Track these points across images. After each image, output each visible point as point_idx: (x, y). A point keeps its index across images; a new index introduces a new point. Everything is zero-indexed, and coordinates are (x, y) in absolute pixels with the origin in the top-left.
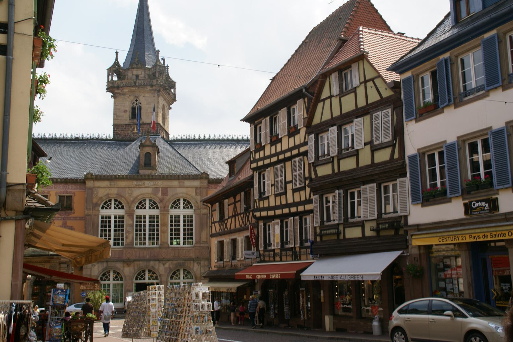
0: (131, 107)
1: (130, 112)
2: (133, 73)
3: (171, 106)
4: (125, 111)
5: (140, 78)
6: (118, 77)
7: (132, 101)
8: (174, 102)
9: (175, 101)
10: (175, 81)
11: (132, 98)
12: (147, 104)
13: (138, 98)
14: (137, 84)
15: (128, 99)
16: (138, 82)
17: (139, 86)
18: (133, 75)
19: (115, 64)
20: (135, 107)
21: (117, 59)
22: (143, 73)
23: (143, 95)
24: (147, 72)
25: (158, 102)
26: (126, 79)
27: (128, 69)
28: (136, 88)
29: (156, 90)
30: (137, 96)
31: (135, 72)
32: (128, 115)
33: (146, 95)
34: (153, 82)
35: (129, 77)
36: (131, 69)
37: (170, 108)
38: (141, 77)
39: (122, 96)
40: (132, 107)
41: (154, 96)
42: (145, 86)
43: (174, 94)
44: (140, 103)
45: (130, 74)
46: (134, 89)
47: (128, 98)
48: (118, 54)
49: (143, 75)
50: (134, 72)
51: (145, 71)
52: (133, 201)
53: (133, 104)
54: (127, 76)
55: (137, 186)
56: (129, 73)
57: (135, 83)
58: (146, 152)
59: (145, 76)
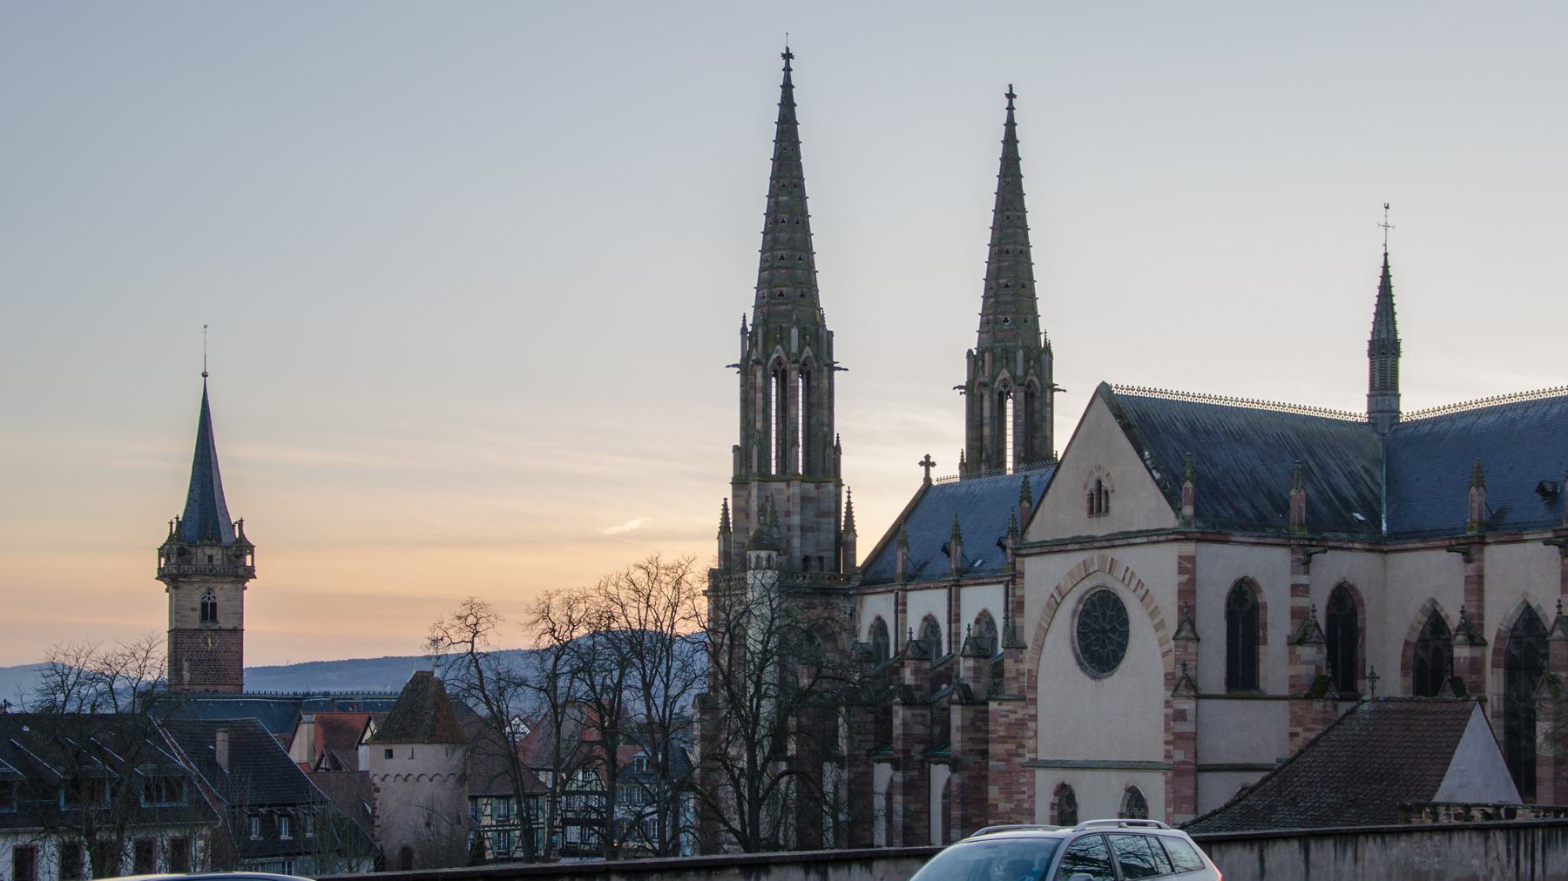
4: (194, 610)
5: (215, 562)
12: (227, 601)
18: (204, 555)
22: (220, 553)
31: (208, 551)
33: (226, 586)
39: (188, 587)
41: (237, 590)
44: (214, 597)
45: (200, 554)
49: (219, 557)
50: (206, 550)
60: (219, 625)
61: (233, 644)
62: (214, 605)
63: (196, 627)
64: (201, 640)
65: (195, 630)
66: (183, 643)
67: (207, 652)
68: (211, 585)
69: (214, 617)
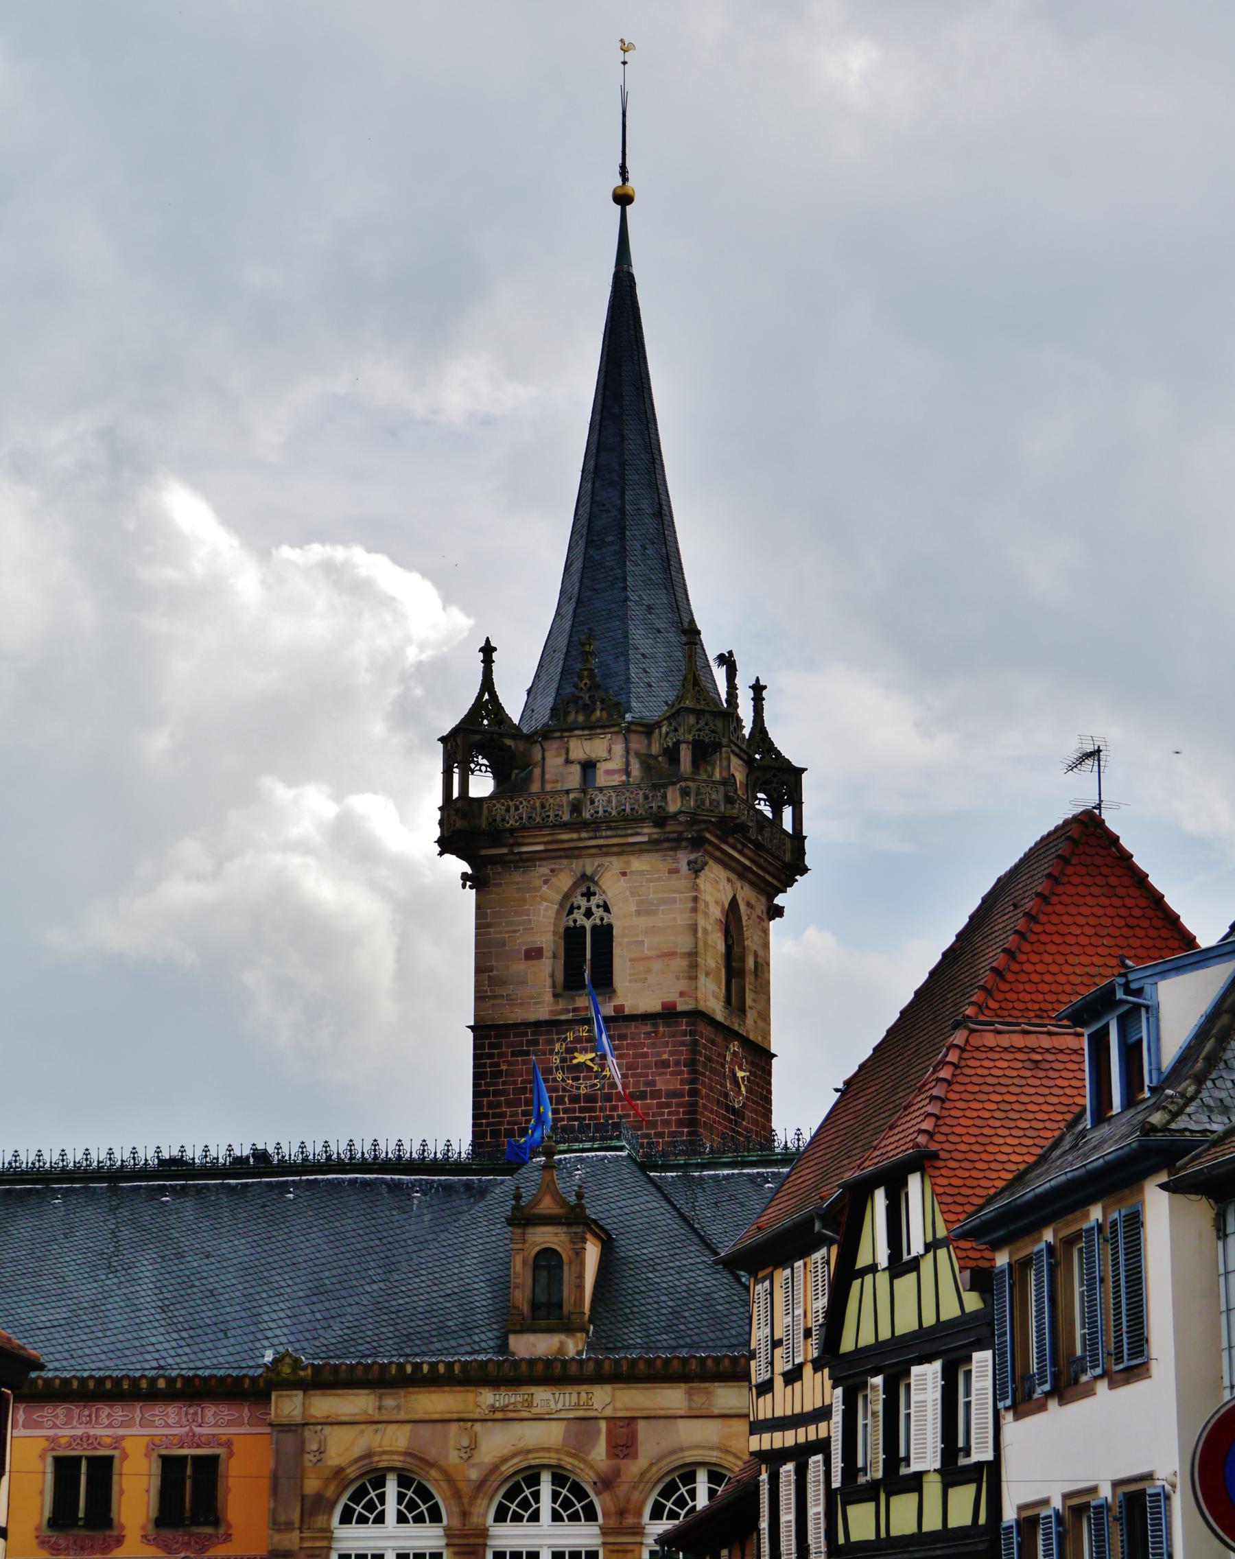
0: (562, 930)
1: (555, 956)
2: (567, 753)
3: (779, 900)
4: (534, 954)
5: (602, 780)
6: (500, 775)
7: (566, 896)
8: (798, 877)
9: (804, 870)
10: (796, 763)
11: (565, 881)
12: (638, 913)
13: (596, 883)
14: (587, 815)
15: (545, 888)
16: (592, 802)
17: (593, 825)
18: (568, 762)
19: (478, 704)
20: (583, 928)
21: (487, 683)
22: (619, 748)
23: (616, 863)
24: (637, 743)
25: (695, 899)
26: (535, 787)
27: (545, 734)
28: (584, 835)
29: (679, 839)
30: (589, 872)
31: (580, 749)
32: (548, 970)
33: (638, 863)
34: (664, 797)
35: (547, 777)
36: (558, 734)
37: (778, 912)
38: (609, 772)
40: (567, 929)
41: (676, 871)
42: (628, 820)
43: (798, 838)
44: (606, 908)
45: (554, 761)
46: (575, 836)
47: (546, 882)
48: (495, 656)
49: (617, 763)
51: (627, 741)
52: (481, 1485)
53: (571, 912)
54: (537, 771)
55: (499, 1415)
56: (547, 754)
57: (576, 808)
58: (538, 1249)
59: (628, 764)
60: (617, 1002)
61: (665, 1064)
62: (604, 935)
63: (542, 1013)
64: (556, 1060)
65: (538, 1024)
66: (499, 1074)
67: (575, 1099)
68: (589, 866)
69: (604, 980)
